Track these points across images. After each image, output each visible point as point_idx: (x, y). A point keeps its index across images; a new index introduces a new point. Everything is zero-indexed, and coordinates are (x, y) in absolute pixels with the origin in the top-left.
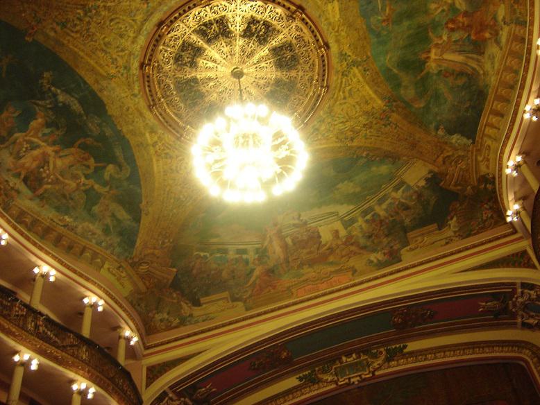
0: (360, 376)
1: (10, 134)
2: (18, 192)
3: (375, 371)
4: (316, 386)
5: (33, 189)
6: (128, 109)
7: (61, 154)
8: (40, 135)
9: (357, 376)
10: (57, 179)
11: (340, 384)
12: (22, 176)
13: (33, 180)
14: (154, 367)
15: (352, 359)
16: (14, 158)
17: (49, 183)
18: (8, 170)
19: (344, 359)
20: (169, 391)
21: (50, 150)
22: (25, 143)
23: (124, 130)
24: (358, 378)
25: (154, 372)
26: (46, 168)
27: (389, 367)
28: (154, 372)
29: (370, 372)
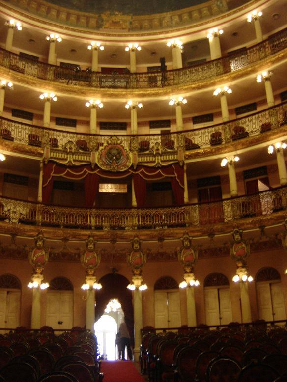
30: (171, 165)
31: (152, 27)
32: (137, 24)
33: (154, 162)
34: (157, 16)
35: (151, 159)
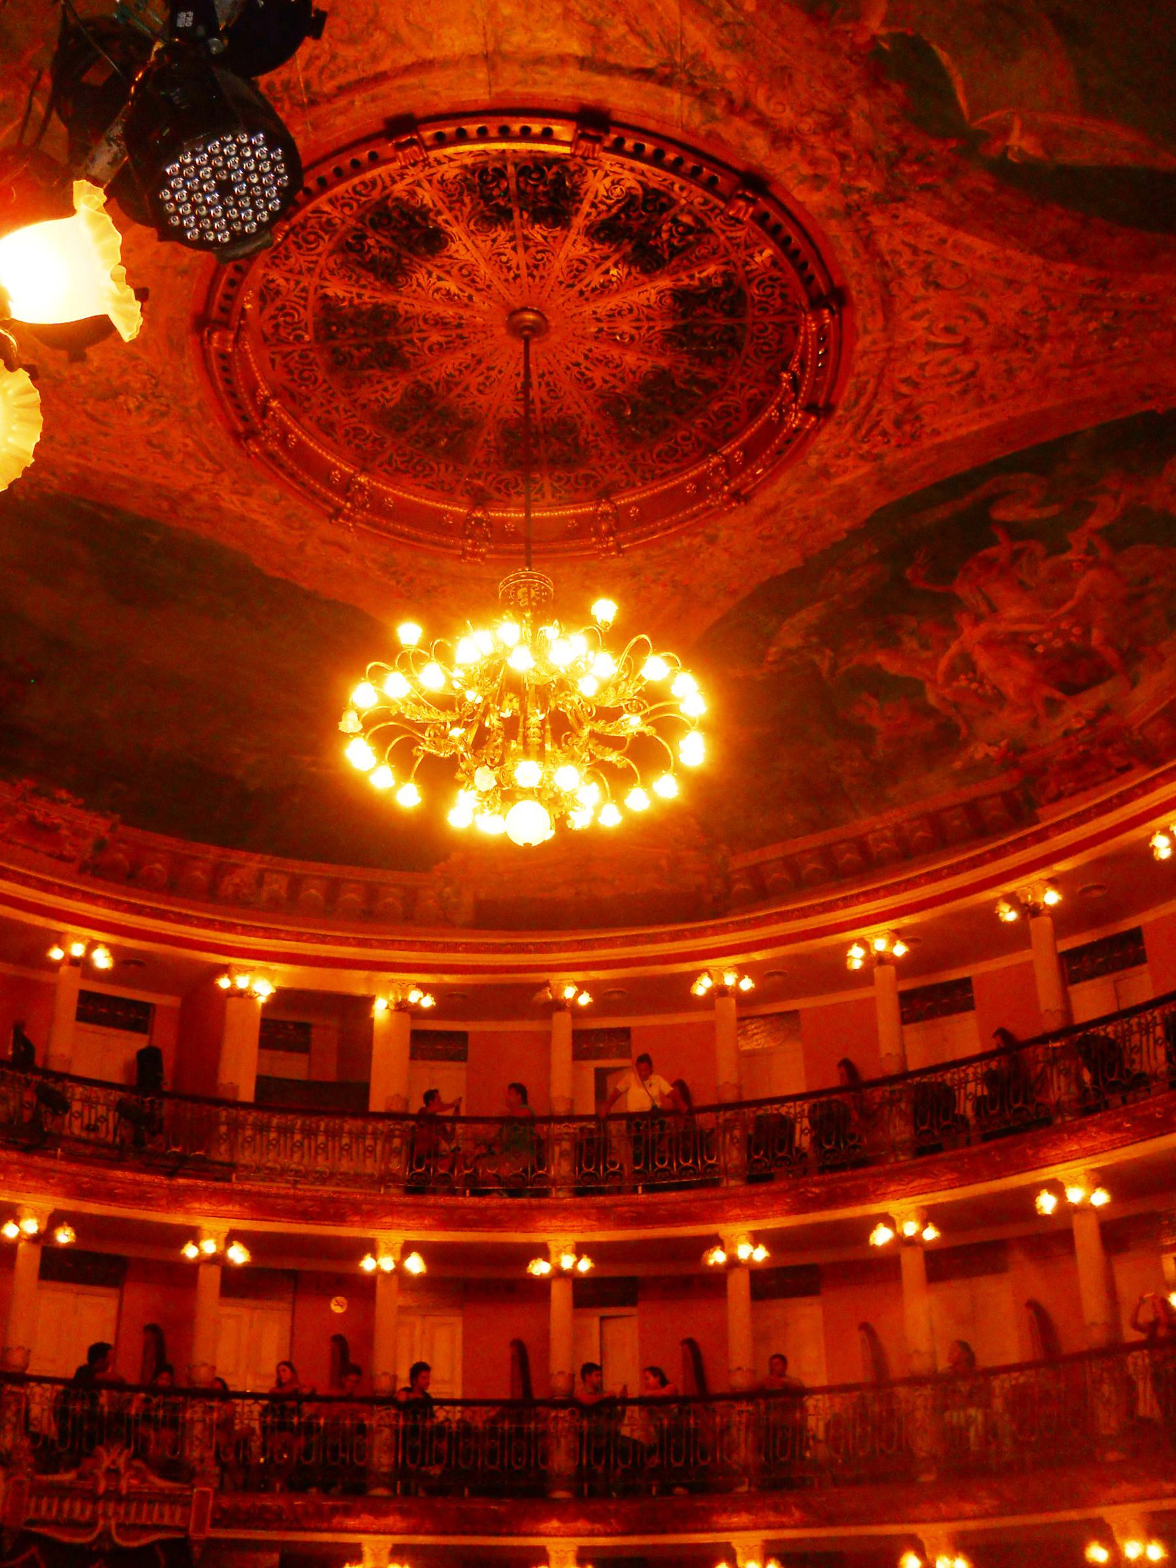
1: (931, 712)
2: (1104, 711)
5: (1100, 674)
6: (769, 538)
7: (983, 609)
8: (925, 655)
10: (1071, 613)
12: (1058, 695)
13: (1071, 671)
16: (1001, 709)
17: (1086, 634)
18: (1035, 724)
21: (971, 635)
22: (955, 684)
23: (846, 525)
26: (1032, 639)
30: (149, 1548)
31: (177, 889)
32: (120, 856)
33: (91, 1525)
34: (213, 854)
35: (80, 1510)
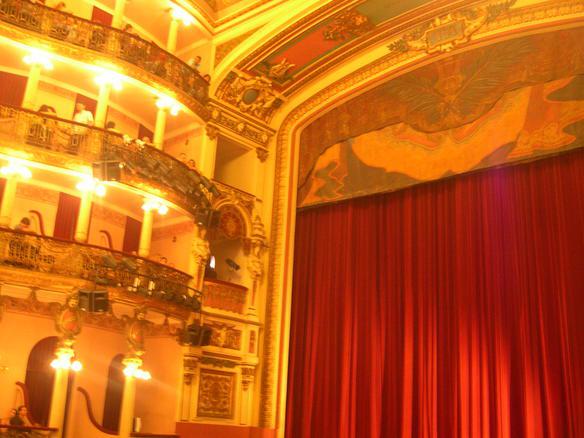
0: (453, 43)
3: (469, 36)
4: (405, 55)
9: (448, 43)
11: (430, 52)
14: (222, 46)
15: (446, 21)
19: (438, 21)
20: (236, 71)
24: (450, 45)
25: (223, 50)
27: (488, 30)
28: (223, 50)
29: (464, 36)
